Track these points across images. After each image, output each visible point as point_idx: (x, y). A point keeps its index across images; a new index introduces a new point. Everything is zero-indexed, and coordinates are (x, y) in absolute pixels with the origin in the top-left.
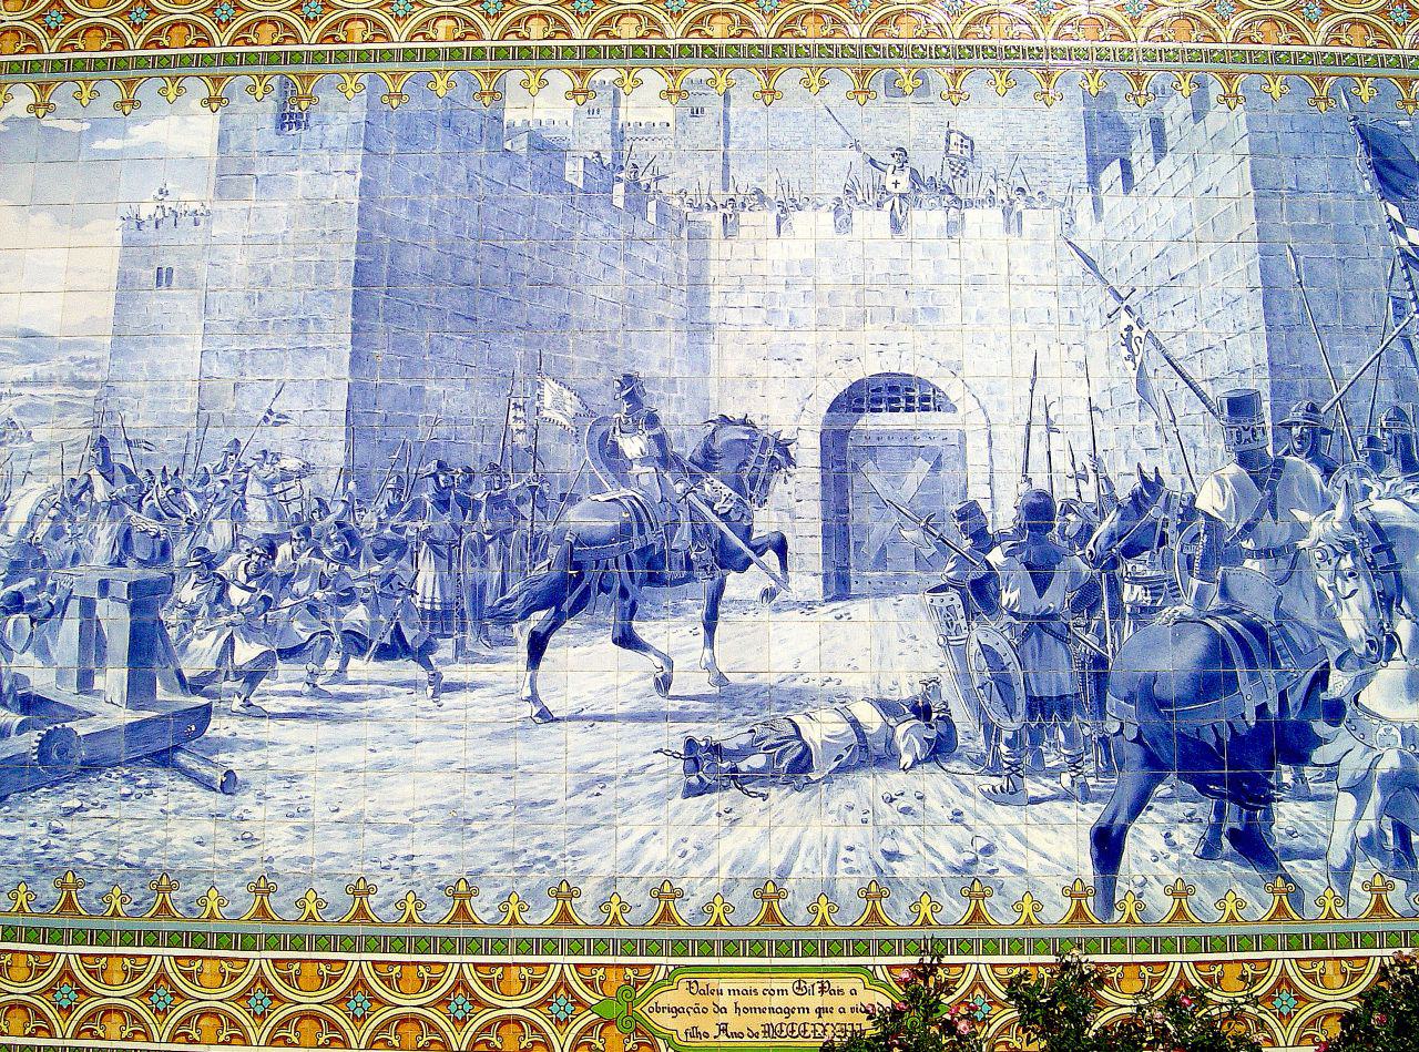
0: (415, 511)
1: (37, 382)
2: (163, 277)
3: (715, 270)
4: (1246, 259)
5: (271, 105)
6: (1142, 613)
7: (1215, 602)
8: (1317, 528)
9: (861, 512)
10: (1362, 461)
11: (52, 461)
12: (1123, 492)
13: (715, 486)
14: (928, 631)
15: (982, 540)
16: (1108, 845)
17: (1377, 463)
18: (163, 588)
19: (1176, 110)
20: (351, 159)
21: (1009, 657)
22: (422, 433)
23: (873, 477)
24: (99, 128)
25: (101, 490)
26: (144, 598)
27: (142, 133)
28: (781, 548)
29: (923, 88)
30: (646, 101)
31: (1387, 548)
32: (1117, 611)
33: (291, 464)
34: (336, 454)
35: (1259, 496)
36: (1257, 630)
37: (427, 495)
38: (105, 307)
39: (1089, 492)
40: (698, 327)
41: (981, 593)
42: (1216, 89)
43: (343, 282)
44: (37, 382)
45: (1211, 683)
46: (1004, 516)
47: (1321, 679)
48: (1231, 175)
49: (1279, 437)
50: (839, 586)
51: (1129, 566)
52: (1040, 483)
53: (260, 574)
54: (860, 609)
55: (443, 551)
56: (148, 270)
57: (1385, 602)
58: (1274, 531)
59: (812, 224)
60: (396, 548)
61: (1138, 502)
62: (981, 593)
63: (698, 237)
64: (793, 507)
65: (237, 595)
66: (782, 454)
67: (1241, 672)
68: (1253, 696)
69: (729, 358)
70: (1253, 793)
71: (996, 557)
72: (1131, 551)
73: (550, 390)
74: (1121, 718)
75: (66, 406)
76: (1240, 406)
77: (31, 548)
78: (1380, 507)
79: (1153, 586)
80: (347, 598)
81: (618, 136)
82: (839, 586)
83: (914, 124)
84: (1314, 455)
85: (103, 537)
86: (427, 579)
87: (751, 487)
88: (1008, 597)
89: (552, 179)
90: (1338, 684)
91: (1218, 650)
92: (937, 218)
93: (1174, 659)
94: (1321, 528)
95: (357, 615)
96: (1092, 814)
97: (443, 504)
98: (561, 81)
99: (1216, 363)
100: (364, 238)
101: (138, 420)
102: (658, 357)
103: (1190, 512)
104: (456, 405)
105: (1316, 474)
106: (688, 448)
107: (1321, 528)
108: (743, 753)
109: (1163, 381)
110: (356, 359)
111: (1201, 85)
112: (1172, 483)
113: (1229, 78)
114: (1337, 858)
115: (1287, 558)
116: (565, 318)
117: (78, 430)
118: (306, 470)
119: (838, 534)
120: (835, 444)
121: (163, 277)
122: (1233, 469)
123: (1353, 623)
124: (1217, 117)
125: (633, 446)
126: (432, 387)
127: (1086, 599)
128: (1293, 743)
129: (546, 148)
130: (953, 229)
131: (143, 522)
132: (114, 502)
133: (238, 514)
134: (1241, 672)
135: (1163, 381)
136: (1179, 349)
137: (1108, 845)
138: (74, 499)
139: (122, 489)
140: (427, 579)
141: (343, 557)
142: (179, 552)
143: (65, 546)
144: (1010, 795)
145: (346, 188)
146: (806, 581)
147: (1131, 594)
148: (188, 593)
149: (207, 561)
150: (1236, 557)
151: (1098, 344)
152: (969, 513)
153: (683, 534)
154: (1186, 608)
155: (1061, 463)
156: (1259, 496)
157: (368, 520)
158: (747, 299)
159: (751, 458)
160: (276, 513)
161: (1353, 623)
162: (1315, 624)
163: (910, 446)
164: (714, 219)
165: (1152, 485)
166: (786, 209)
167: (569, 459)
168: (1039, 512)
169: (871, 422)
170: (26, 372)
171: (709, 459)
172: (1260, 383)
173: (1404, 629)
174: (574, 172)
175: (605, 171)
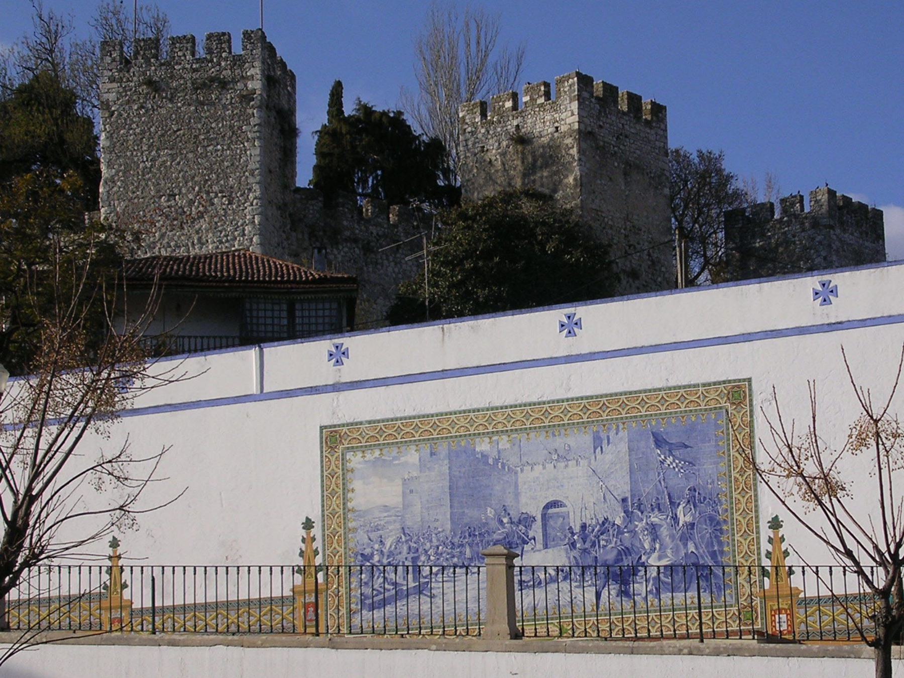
0: (465, 538)
1: (388, 516)
2: (411, 491)
3: (520, 480)
4: (626, 467)
5: (429, 451)
6: (605, 546)
7: (619, 543)
8: (640, 525)
9: (549, 530)
10: (649, 510)
11: (393, 533)
12: (600, 522)
13: (521, 527)
14: (563, 554)
15: (573, 534)
16: (598, 595)
17: (653, 510)
18: (418, 558)
19: (612, 434)
20: (446, 462)
21: (578, 558)
22: (465, 521)
23: (551, 522)
24: (395, 458)
25: (404, 539)
26: (415, 560)
27: (403, 459)
28: (534, 539)
29: (560, 435)
30: (504, 442)
31: (654, 528)
32: (599, 547)
33: (440, 530)
34: (449, 526)
35: (628, 520)
36: (627, 548)
37: (467, 535)
38: (400, 499)
39: (594, 522)
40: (517, 495)
41: (573, 545)
42: (621, 426)
43: (447, 490)
44: (388, 516)
45: (618, 559)
46: (577, 529)
47: (640, 558)
48: (624, 447)
49: (632, 506)
50: (546, 546)
51: (601, 537)
52: (584, 521)
53: (436, 553)
54: (550, 550)
55: (471, 546)
56: (408, 489)
57: (654, 540)
58: (631, 526)
59: (538, 468)
60: (462, 545)
61: (603, 523)
62: (573, 545)
63: (516, 473)
64: (536, 530)
65: (432, 558)
66: (534, 519)
67: (624, 557)
68: (627, 562)
69: (523, 499)
71: (576, 537)
72: (602, 534)
73: (489, 509)
75: (395, 521)
76: (624, 500)
77: (391, 552)
78: (653, 520)
79: (607, 541)
80: (453, 557)
81: (499, 452)
82: (546, 546)
83: (558, 442)
84: (639, 510)
85: (405, 549)
86: (468, 552)
87: (528, 527)
88: (578, 545)
89: (486, 463)
90: (644, 558)
92: (563, 464)
93: (611, 557)
94: (640, 525)
95: (455, 560)
97: (470, 536)
98: (487, 440)
99: (619, 491)
100: (450, 479)
101: (409, 523)
102: (509, 502)
103: (614, 524)
104: (472, 514)
105: (640, 514)
106: (516, 520)
107: (640, 525)
108: (529, 581)
109: (609, 496)
110: (451, 507)
111: (618, 426)
112: (610, 519)
113: (624, 423)
115: (633, 533)
116: (491, 494)
117: (398, 526)
118: (443, 531)
119: (545, 535)
120: (544, 516)
121: (411, 491)
122: (623, 514)
123: (647, 546)
124: (621, 434)
125: (505, 520)
126: (466, 511)
127: (593, 545)
128: (633, 571)
129: (485, 456)
130: (566, 466)
131: (413, 545)
132: (407, 541)
133: (431, 541)
134: (624, 557)
135: (609, 496)
136: (612, 489)
137: (598, 595)
138: (399, 541)
139: (408, 538)
140: (468, 550)
141: (452, 548)
142: (420, 550)
143: (398, 551)
145: (445, 469)
146: (539, 546)
147: (602, 543)
148: (423, 558)
149: (426, 552)
150: (623, 533)
151: (595, 490)
152: (571, 528)
153: (516, 538)
154: (613, 545)
155: (588, 516)
156: (628, 520)
157: (456, 540)
158: (526, 487)
159: (526, 520)
160: (438, 540)
161: (647, 546)
163: (558, 515)
164: (519, 469)
165: (606, 519)
166: (532, 466)
167: (494, 524)
168: (584, 527)
169: (551, 511)
170: (386, 514)
171: (520, 522)
172: (628, 495)
173: (657, 546)
174: (491, 461)
175: (496, 461)
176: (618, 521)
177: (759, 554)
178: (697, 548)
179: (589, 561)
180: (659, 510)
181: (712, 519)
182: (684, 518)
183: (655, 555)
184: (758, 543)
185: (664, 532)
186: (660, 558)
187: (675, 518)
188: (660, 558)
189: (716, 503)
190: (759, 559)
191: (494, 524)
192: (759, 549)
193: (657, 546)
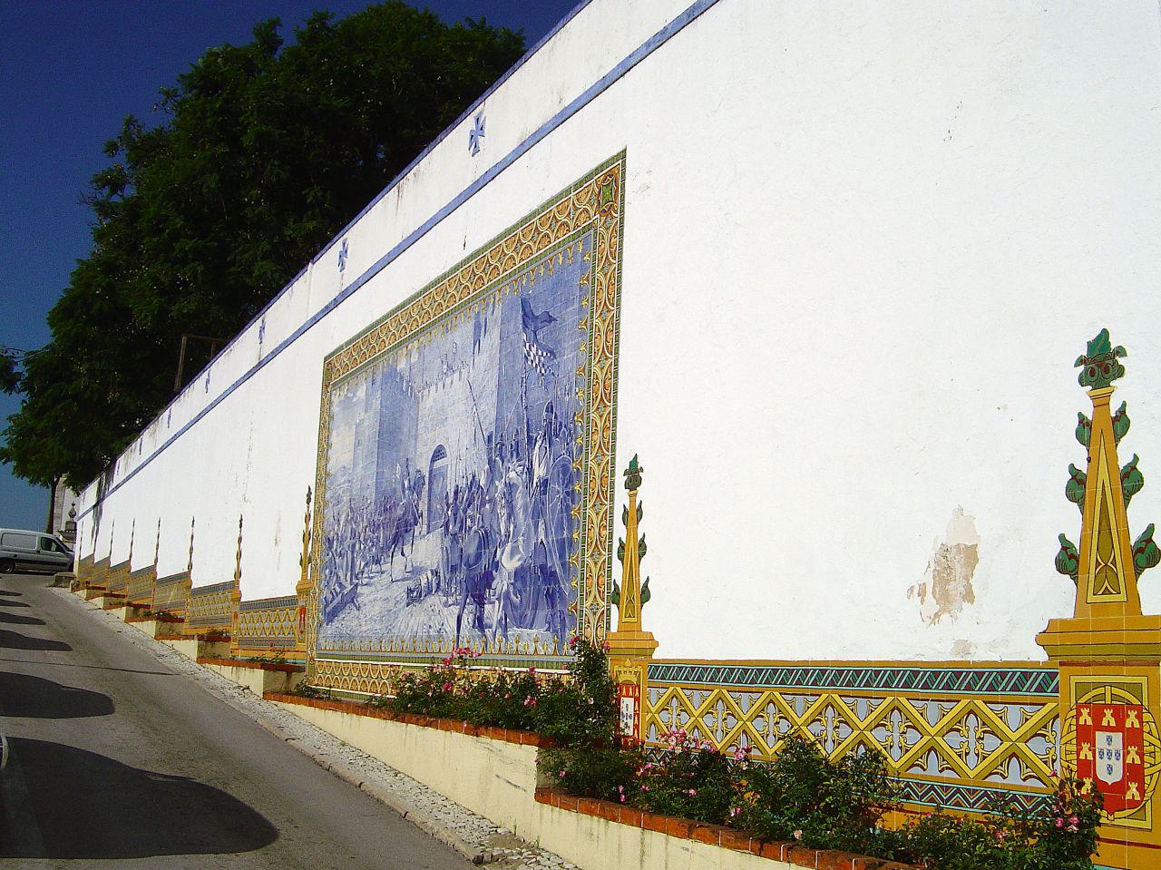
45: (478, 557)
49: (499, 448)
70: (480, 602)
74: (461, 575)
87: (419, 494)
91: (479, 547)
93: (472, 550)
96: (456, 610)
114: (494, 628)
127: (461, 528)
128: (488, 579)
135: (479, 435)
144: (446, 605)
162: (496, 529)
168: (456, 493)
176: (482, 483)
177: (610, 551)
178: (546, 536)
179: (456, 560)
180: (518, 454)
181: (565, 469)
182: (539, 472)
183: (508, 548)
184: (611, 525)
185: (519, 501)
186: (512, 555)
187: (530, 471)
188: (512, 555)
189: (572, 435)
190: (610, 558)
191: (399, 493)
192: (611, 534)
193: (512, 526)
